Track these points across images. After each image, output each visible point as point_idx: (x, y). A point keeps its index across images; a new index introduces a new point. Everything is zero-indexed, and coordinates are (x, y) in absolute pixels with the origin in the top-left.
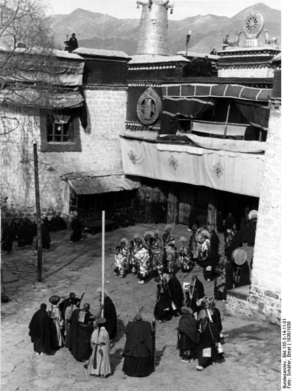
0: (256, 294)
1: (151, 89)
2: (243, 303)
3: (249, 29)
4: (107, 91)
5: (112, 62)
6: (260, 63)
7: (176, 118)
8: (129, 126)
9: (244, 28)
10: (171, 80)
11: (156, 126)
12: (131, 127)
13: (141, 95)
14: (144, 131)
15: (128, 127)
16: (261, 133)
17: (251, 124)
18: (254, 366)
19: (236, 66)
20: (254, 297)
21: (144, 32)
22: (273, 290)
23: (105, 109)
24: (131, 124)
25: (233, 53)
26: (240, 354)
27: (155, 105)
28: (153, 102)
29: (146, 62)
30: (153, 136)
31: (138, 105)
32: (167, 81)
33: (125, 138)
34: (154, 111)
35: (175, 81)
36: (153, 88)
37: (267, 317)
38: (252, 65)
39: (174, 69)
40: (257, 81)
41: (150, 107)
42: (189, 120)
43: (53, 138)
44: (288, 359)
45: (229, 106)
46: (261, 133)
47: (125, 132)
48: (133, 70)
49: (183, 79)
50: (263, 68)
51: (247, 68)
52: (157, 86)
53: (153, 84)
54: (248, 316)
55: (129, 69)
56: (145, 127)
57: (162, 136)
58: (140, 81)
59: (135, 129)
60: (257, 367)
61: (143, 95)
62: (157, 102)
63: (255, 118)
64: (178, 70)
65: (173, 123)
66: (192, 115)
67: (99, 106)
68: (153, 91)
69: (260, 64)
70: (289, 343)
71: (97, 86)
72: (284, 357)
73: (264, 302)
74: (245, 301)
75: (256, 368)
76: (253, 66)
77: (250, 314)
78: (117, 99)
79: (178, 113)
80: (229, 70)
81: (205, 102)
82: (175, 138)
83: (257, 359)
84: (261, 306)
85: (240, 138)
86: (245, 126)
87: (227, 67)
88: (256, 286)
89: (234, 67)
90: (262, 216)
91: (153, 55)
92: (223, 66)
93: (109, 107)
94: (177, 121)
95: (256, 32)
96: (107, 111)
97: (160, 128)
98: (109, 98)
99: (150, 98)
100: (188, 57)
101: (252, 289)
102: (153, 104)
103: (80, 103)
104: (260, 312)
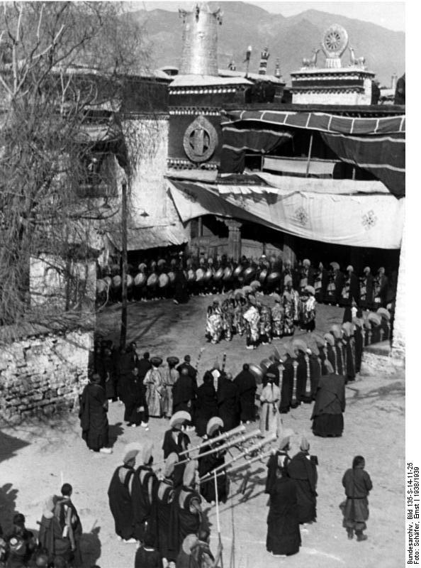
1: (203, 118)
3: (329, 46)
8: (173, 164)
9: (323, 44)
10: (233, 106)
12: (175, 166)
15: (171, 165)
16: (354, 171)
19: (316, 90)
21: (189, 47)
25: (312, 75)
27: (208, 136)
28: (206, 133)
30: (211, 175)
31: (185, 138)
34: (207, 145)
36: (206, 117)
39: (234, 93)
42: (259, 155)
47: (168, 172)
48: (176, 95)
52: (211, 114)
53: (205, 112)
55: (171, 93)
56: (196, 165)
57: (223, 175)
58: (187, 107)
59: (180, 168)
62: (211, 134)
65: (237, 159)
66: (264, 149)
68: (206, 120)
72: (410, 518)
76: (339, 91)
79: (245, 148)
80: (307, 94)
81: (280, 134)
82: (241, 177)
86: (334, 162)
91: (202, 75)
92: (298, 90)
95: (339, 49)
100: (250, 79)
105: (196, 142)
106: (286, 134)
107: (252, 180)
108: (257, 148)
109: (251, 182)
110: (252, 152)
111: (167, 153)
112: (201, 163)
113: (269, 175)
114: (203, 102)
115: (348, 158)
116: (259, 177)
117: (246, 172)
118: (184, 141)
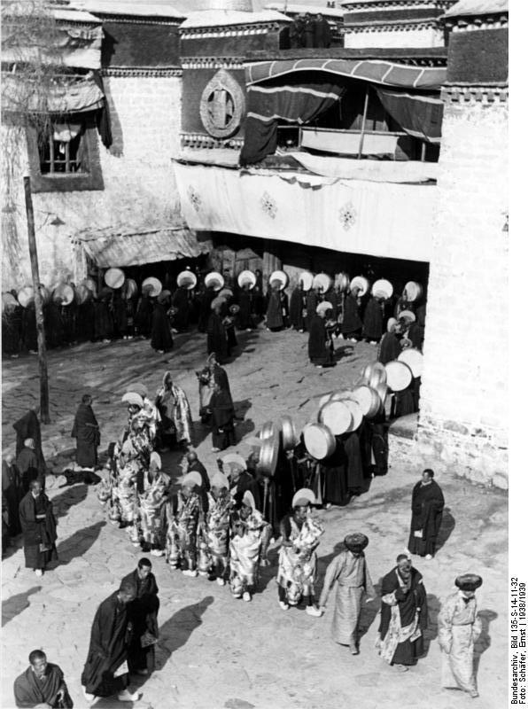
0: (428, 428)
2: (406, 445)
4: (144, 79)
5: (152, 25)
6: (418, 20)
7: (272, 124)
8: (188, 141)
10: (261, 55)
11: (236, 140)
13: (206, 84)
14: (214, 150)
15: (186, 143)
16: (424, 146)
20: (425, 432)
22: (459, 420)
24: (191, 138)
27: (232, 102)
28: (228, 96)
29: (213, 23)
31: (202, 102)
32: (252, 58)
33: (182, 162)
34: (231, 113)
35: (268, 57)
36: (229, 71)
37: (448, 467)
38: (404, 25)
39: (264, 35)
40: (415, 53)
41: (224, 105)
42: (296, 127)
43: (52, 167)
44: (520, 650)
45: (367, 97)
49: (282, 52)
50: (424, 28)
51: (396, 30)
52: (235, 67)
53: (228, 64)
55: (183, 37)
58: (204, 58)
59: (199, 147)
61: (210, 83)
62: (236, 97)
63: (413, 122)
64: (272, 38)
65: (266, 134)
69: (419, 23)
70: (522, 621)
71: (126, 69)
72: (514, 646)
73: (443, 441)
74: (410, 440)
77: (419, 462)
79: (276, 116)
80: (364, 33)
84: (439, 448)
85: (386, 157)
86: (396, 136)
87: (359, 29)
88: (428, 414)
89: (373, 28)
91: (225, 11)
92: (352, 28)
94: (273, 130)
96: (147, 116)
97: (243, 143)
98: (150, 91)
100: (289, 14)
101: (421, 419)
102: (230, 101)
103: (97, 102)
104: (437, 458)
105: (216, 109)
106: (332, 95)
108: (292, 118)
109: (283, 166)
110: (285, 123)
111: (180, 125)
112: (224, 138)
113: (308, 155)
114: (224, 51)
117: (280, 152)
118: (201, 108)
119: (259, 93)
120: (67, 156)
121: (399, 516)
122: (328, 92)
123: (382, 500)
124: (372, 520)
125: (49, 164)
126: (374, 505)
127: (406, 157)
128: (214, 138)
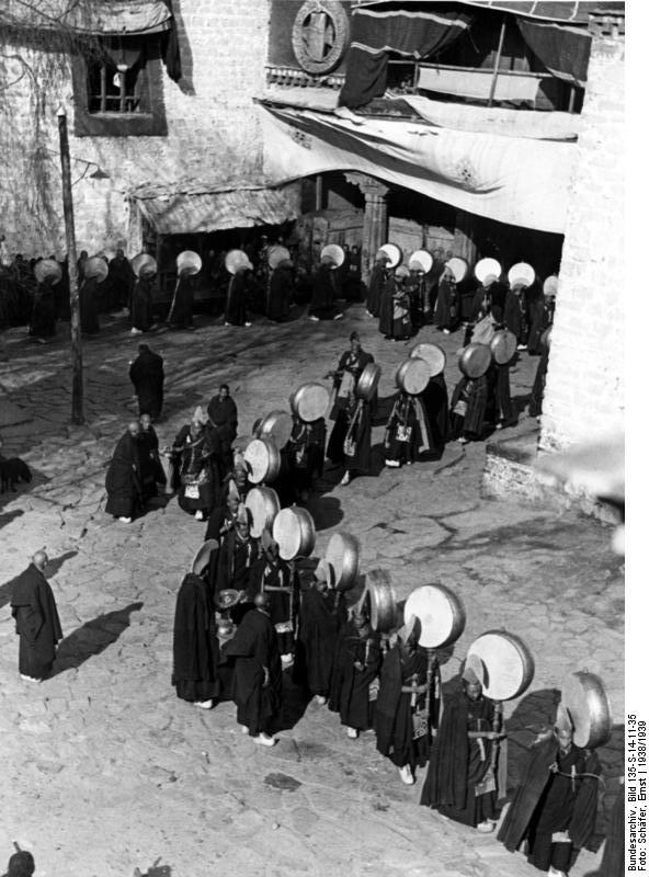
2: (522, 472)
7: (381, 58)
8: (276, 76)
11: (336, 77)
12: (279, 80)
14: (308, 89)
15: (273, 79)
16: (573, 92)
17: (549, 72)
18: (541, 603)
23: (219, 37)
24: (279, 73)
26: (513, 579)
27: (333, 27)
28: (328, 20)
30: (329, 98)
31: (295, 27)
33: (266, 104)
34: (330, 42)
37: (574, 502)
42: (412, 62)
44: (640, 804)
45: (504, 27)
46: (573, 92)
47: (266, 91)
54: (533, 499)
59: (288, 84)
60: (546, 604)
62: (338, 21)
65: (372, 71)
66: (419, 50)
67: (206, 28)
75: (544, 607)
77: (537, 494)
78: (247, 14)
79: (387, 48)
83: (549, 589)
85: (524, 105)
86: (538, 77)
88: (551, 434)
90: (568, 253)
93: (228, 31)
94: (382, 65)
97: (344, 81)
98: (230, 11)
99: (322, 12)
101: (542, 440)
102: (330, 27)
103: (162, 23)
104: (559, 490)
105: (313, 36)
106: (458, 23)
107: (397, 110)
108: (407, 51)
109: (393, 113)
110: (398, 57)
111: (266, 55)
112: (321, 75)
113: (425, 99)
115: (563, 71)
116: (406, 103)
117: (390, 95)
118: (294, 34)
119: (368, 17)
120: (122, 91)
121: (506, 561)
122: (455, 19)
123: (487, 540)
124: (469, 564)
125: (100, 100)
126: (475, 546)
127: (551, 106)
128: (309, 74)
